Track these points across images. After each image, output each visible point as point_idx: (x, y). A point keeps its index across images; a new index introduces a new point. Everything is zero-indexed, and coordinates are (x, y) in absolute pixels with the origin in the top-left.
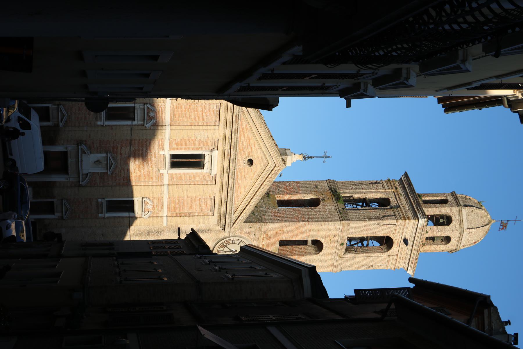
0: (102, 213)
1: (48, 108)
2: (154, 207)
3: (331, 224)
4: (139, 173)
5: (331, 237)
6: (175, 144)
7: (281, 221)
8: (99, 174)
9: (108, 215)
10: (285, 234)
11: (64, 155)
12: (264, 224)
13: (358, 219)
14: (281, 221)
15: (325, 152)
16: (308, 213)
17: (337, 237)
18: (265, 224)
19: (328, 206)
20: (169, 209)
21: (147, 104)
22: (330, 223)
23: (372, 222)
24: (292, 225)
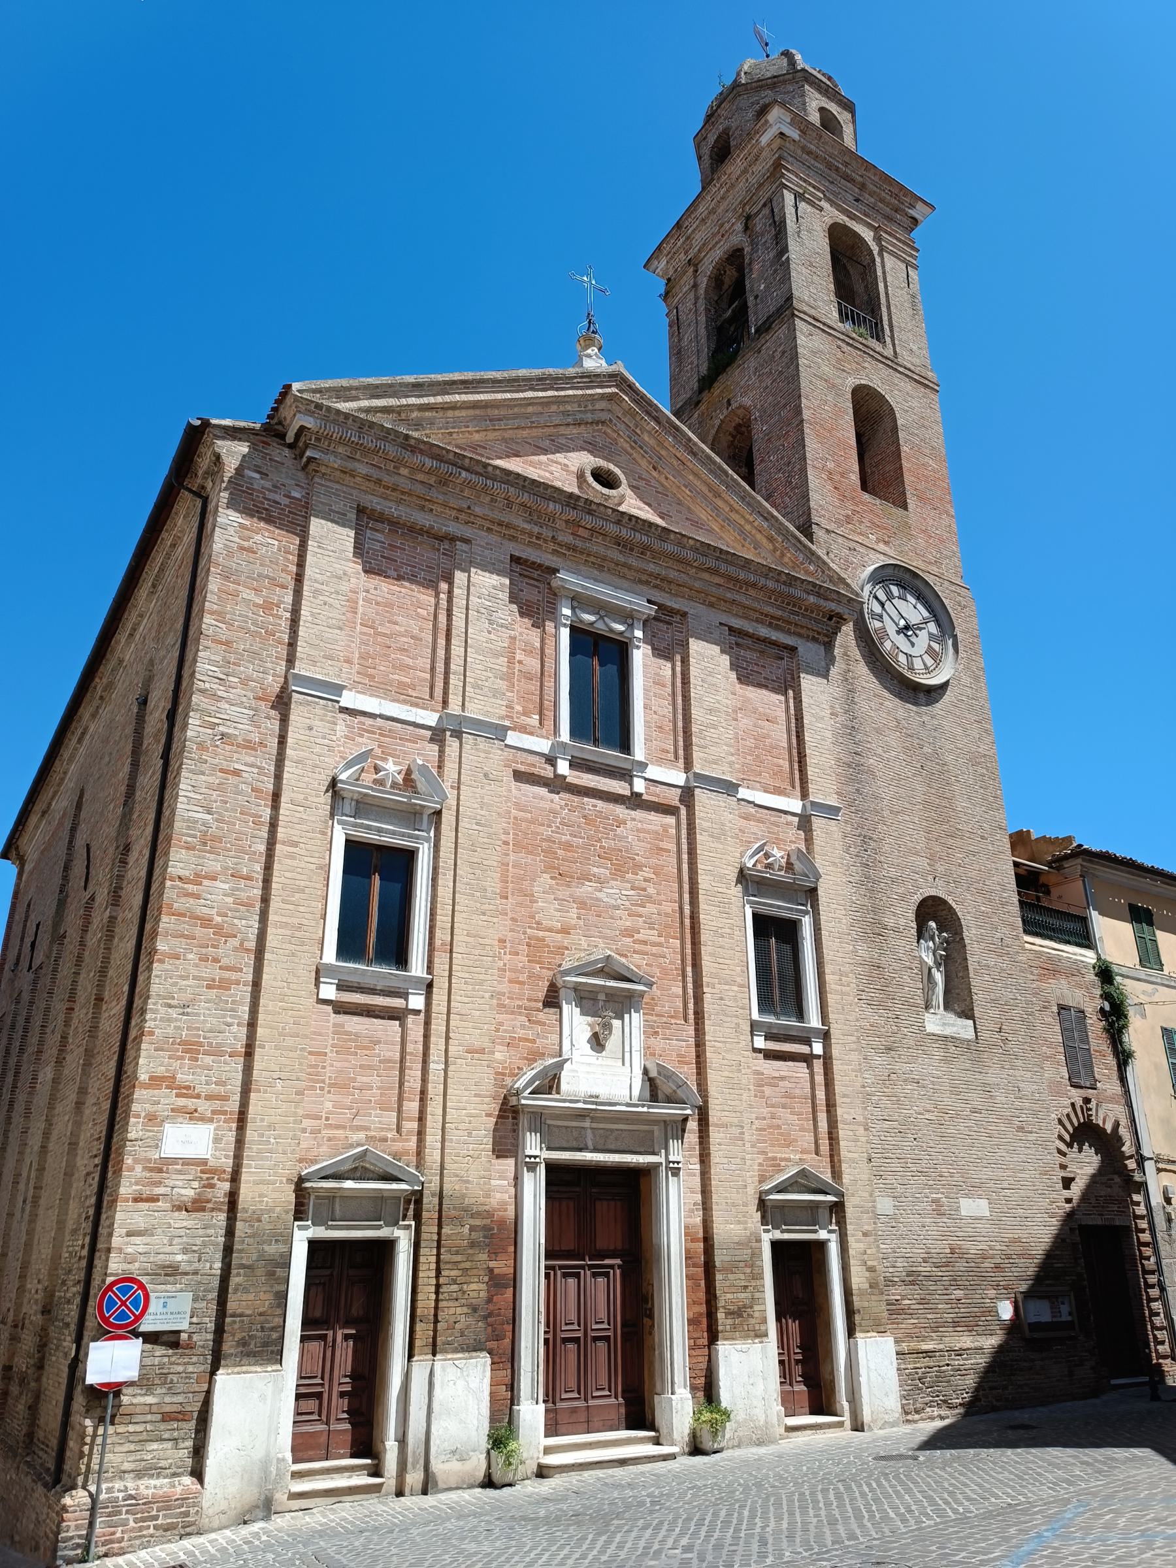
1: (315, 1246)
2: (778, 842)
3: (801, 340)
4: (647, 873)
6: (526, 713)
7: (803, 470)
8: (651, 1032)
11: (560, 1179)
12: (815, 519)
17: (839, 343)
19: (746, 385)
24: (813, 446)
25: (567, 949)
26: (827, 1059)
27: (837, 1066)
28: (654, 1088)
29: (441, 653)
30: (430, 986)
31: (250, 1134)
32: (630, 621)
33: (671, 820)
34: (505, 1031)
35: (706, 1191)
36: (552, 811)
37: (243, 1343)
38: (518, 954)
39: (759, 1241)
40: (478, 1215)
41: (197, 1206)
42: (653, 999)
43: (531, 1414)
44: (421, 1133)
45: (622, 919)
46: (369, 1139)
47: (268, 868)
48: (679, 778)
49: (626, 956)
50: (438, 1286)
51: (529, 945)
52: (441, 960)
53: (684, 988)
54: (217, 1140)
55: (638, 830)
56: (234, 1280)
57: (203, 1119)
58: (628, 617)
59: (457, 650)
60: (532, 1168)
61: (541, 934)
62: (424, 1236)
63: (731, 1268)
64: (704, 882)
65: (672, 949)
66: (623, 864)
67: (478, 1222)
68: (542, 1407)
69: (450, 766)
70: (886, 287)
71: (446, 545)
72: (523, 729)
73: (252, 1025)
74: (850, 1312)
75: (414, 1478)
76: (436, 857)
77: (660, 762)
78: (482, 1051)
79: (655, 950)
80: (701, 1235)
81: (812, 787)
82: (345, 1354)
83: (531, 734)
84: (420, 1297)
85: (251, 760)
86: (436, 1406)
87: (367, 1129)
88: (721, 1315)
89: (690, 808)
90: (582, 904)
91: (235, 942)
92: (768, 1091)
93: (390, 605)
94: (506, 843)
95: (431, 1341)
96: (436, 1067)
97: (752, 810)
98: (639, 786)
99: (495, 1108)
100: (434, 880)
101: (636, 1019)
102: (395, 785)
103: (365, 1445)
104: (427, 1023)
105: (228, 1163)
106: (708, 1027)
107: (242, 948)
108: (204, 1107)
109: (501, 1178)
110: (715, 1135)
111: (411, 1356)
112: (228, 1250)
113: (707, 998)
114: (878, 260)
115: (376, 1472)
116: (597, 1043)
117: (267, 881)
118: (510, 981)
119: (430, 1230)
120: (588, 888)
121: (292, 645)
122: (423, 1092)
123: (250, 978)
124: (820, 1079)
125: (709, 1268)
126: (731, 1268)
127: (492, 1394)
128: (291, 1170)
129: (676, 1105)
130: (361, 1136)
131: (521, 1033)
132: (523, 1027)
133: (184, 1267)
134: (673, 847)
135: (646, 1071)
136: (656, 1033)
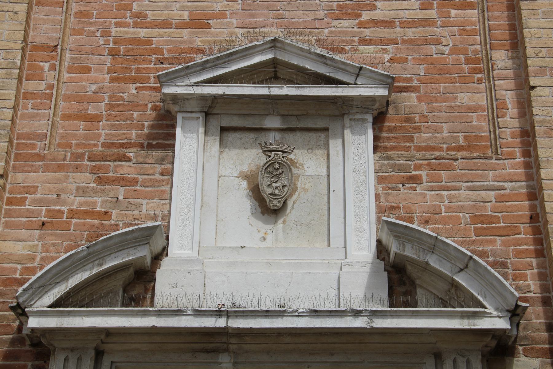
25: (201, 51)
34: (39, 202)
38: (88, 70)
42: (409, 120)
49: (341, 51)
51: (114, 53)
61: (143, 33)
79: (411, 33)
116: (269, 207)
118: (67, 117)
131: (76, 202)
132: (82, 191)
135: (381, 250)
136: (416, 179)
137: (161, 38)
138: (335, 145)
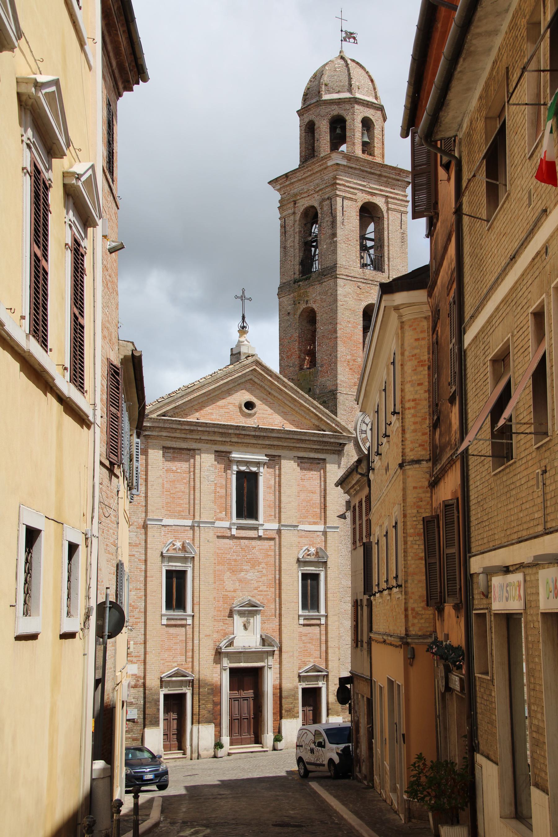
0: (320, 619)
1: (166, 696)
2: (312, 545)
3: (340, 291)
4: (263, 565)
5: (359, 291)
6: (221, 512)
8: (263, 622)
9: (323, 612)
10: (354, 358)
12: (339, 389)
13: (335, 252)
14: (336, 363)
15: (236, 297)
16: (325, 324)
17: (359, 284)
18: (339, 386)
19: (315, 297)
20: (315, 523)
21: (162, 553)
22: (339, 292)
23: (339, 232)
26: (326, 624)
27: (329, 627)
28: (264, 641)
29: (192, 497)
30: (193, 616)
31: (148, 667)
32: (258, 465)
33: (272, 543)
35: (280, 674)
36: (230, 548)
37: (150, 721)
39: (297, 688)
40: (210, 685)
41: (135, 686)
43: (226, 740)
44: (193, 662)
45: (253, 584)
46: (178, 665)
47: (145, 585)
48: (275, 526)
50: (199, 705)
52: (196, 609)
53: (275, 605)
54: (139, 668)
55: (260, 549)
56: (147, 705)
57: (134, 663)
58: (258, 464)
59: (197, 495)
60: (225, 670)
62: (195, 692)
63: (287, 698)
64: (284, 566)
65: (271, 593)
66: (254, 563)
67: (210, 687)
68: (229, 738)
69: (197, 540)
70: (388, 233)
71: (192, 452)
72: (220, 519)
73: (145, 634)
74: (328, 709)
75: (195, 755)
76: (193, 573)
77: (269, 521)
78: (210, 636)
79: (265, 593)
80: (278, 687)
81: (328, 520)
82: (174, 724)
83: (222, 521)
84: (194, 708)
85: (137, 550)
86: (200, 737)
87: (177, 662)
88: (283, 712)
89: (280, 537)
90: (240, 581)
91: (138, 610)
92: (303, 638)
93: (174, 481)
94: (215, 563)
95: (198, 720)
96: (196, 642)
97: (303, 533)
98: (261, 533)
99: (214, 653)
100: (193, 580)
101: (258, 618)
102: (179, 549)
103: (181, 747)
104: (193, 628)
105: (142, 675)
106: (283, 619)
107: (140, 612)
108: (135, 659)
109: (216, 674)
110: (284, 656)
111: (192, 724)
112: (145, 698)
113: (283, 609)
114: (386, 216)
115: (184, 754)
116: (245, 628)
117: (145, 590)
119: (196, 690)
120: (242, 574)
121: (146, 506)
122: (193, 650)
123: (143, 620)
124: (323, 632)
125: (281, 697)
126: (287, 698)
127: (215, 735)
128: (158, 675)
129: (271, 646)
130: (175, 664)
131: (221, 628)
132: (222, 626)
133: (134, 702)
134: (273, 553)
135: (261, 636)
137: (230, 594)
138: (255, 617)
